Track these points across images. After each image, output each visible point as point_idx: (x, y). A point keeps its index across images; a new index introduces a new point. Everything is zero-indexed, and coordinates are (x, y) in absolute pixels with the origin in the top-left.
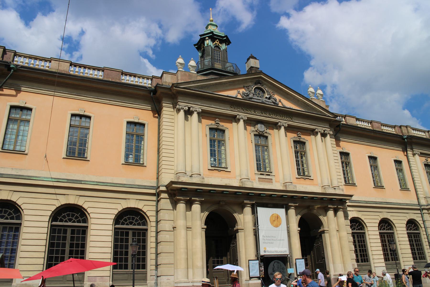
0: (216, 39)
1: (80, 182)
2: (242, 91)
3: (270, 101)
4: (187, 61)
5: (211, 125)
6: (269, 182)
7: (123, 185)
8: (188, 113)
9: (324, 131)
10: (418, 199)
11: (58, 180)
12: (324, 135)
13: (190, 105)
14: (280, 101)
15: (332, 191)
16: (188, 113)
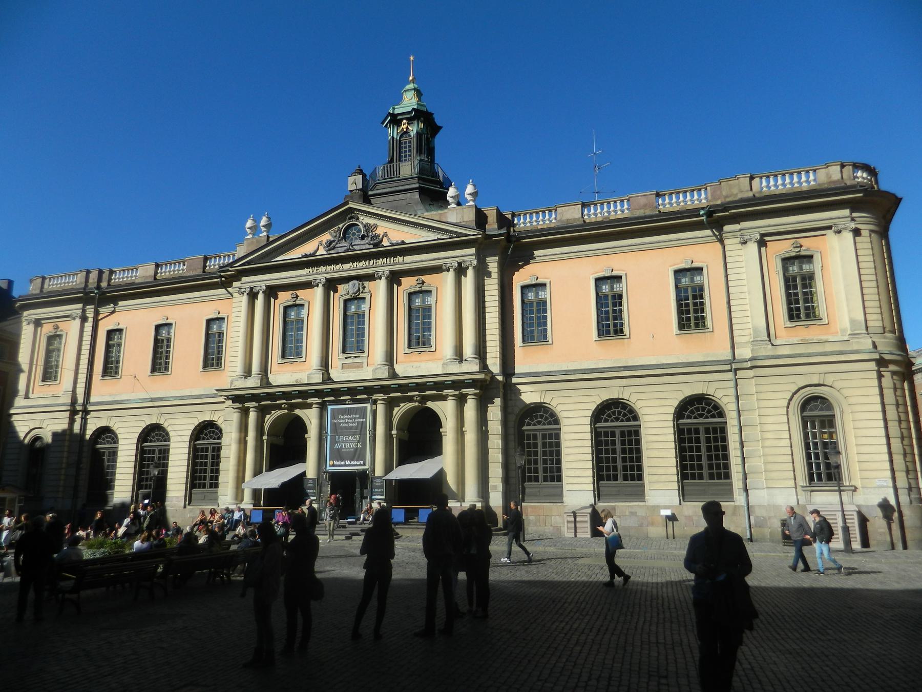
0: (402, 120)
1: (161, 399)
2: (326, 237)
3: (363, 242)
4: (257, 221)
5: (287, 301)
6: (358, 367)
7: (200, 397)
8: (253, 295)
9: (460, 264)
10: (733, 347)
11: (143, 401)
12: (460, 271)
13: (252, 285)
14: (385, 235)
15: (455, 368)
16: (253, 295)
